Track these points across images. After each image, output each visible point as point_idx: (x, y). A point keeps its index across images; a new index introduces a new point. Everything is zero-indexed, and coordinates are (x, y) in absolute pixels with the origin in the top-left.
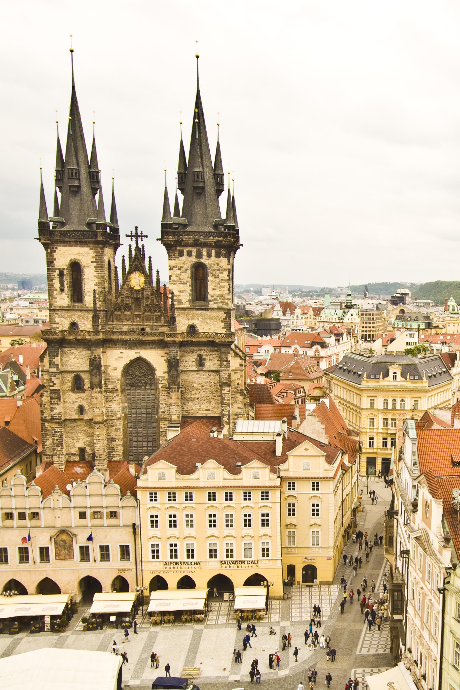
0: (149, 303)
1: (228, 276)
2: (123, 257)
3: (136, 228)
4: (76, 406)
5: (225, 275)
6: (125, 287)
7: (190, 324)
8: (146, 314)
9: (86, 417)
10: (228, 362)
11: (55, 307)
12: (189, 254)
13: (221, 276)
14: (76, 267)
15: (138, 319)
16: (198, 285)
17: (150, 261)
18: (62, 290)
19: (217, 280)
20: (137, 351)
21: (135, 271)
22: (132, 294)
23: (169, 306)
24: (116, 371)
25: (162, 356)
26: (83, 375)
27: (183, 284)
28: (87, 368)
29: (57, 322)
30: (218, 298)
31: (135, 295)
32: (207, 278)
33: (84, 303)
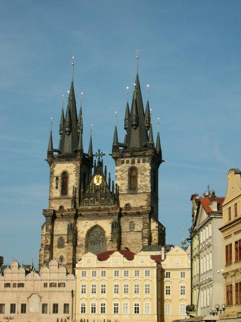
0: (104, 192)
3: (99, 150)
4: (59, 257)
5: (148, 173)
6: (91, 184)
9: (65, 263)
12: (128, 162)
13: (145, 173)
14: (65, 175)
16: (132, 180)
17: (106, 168)
18: (57, 188)
19: (143, 176)
22: (95, 187)
23: (115, 192)
28: (66, 233)
31: (96, 188)
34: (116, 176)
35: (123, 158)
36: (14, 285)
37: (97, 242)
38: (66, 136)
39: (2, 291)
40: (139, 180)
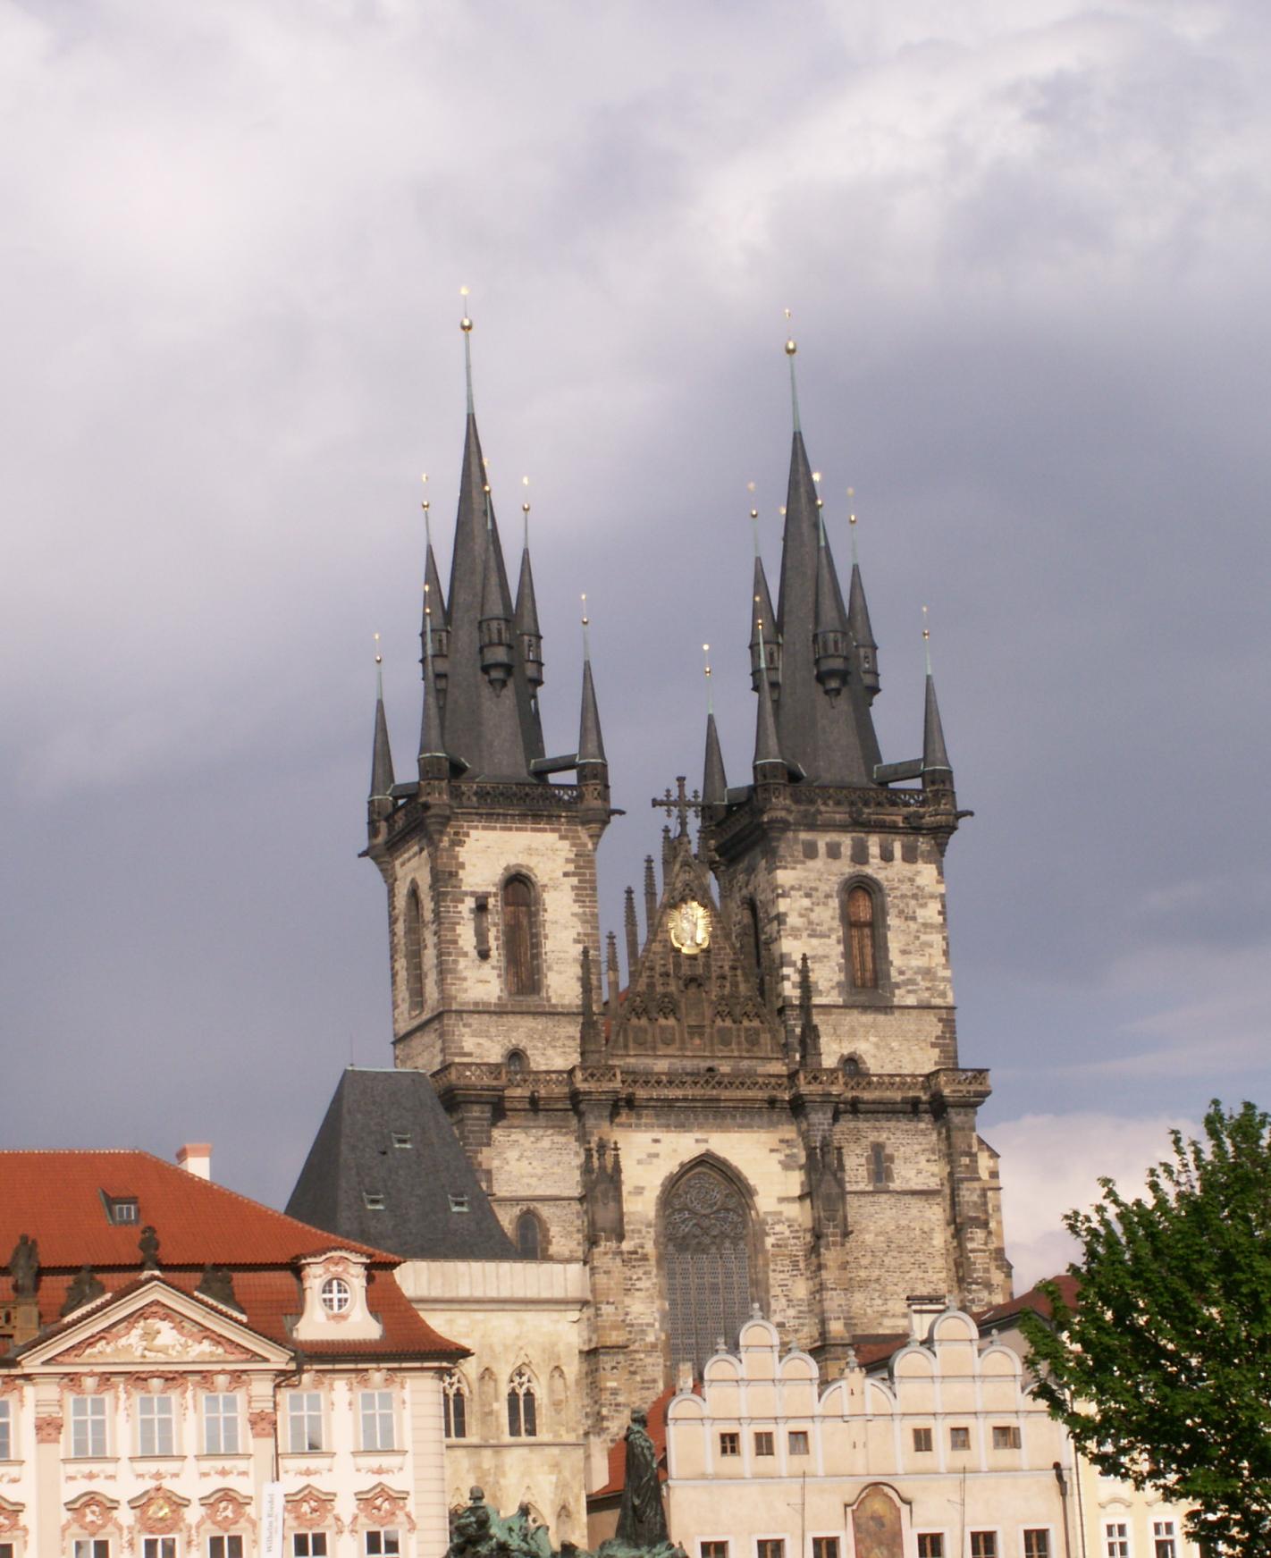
0: (727, 991)
1: (940, 913)
2: (649, 861)
3: (681, 780)
5: (931, 912)
6: (656, 947)
7: (846, 1052)
8: (719, 1022)
10: (973, 1156)
11: (462, 1004)
12: (834, 852)
13: (920, 913)
15: (697, 1041)
16: (855, 943)
20: (698, 1135)
21: (684, 900)
22: (677, 965)
24: (640, 1198)
25: (772, 1151)
26: (545, 1211)
27: (822, 936)
29: (466, 1050)
30: (919, 978)
31: (685, 970)
32: (884, 920)
33: (544, 994)
34: (785, 914)
35: (812, 827)
36: (764, 1444)
37: (707, 1240)
38: (486, 691)
39: (704, 1477)
40: (894, 944)
